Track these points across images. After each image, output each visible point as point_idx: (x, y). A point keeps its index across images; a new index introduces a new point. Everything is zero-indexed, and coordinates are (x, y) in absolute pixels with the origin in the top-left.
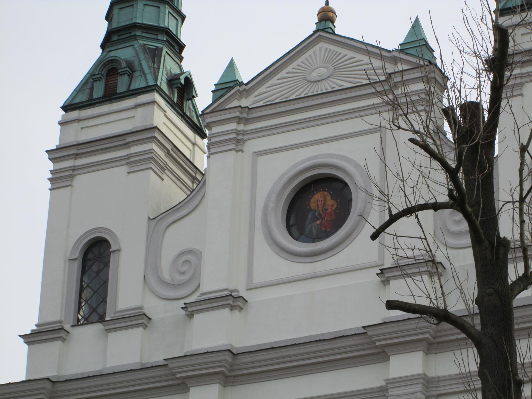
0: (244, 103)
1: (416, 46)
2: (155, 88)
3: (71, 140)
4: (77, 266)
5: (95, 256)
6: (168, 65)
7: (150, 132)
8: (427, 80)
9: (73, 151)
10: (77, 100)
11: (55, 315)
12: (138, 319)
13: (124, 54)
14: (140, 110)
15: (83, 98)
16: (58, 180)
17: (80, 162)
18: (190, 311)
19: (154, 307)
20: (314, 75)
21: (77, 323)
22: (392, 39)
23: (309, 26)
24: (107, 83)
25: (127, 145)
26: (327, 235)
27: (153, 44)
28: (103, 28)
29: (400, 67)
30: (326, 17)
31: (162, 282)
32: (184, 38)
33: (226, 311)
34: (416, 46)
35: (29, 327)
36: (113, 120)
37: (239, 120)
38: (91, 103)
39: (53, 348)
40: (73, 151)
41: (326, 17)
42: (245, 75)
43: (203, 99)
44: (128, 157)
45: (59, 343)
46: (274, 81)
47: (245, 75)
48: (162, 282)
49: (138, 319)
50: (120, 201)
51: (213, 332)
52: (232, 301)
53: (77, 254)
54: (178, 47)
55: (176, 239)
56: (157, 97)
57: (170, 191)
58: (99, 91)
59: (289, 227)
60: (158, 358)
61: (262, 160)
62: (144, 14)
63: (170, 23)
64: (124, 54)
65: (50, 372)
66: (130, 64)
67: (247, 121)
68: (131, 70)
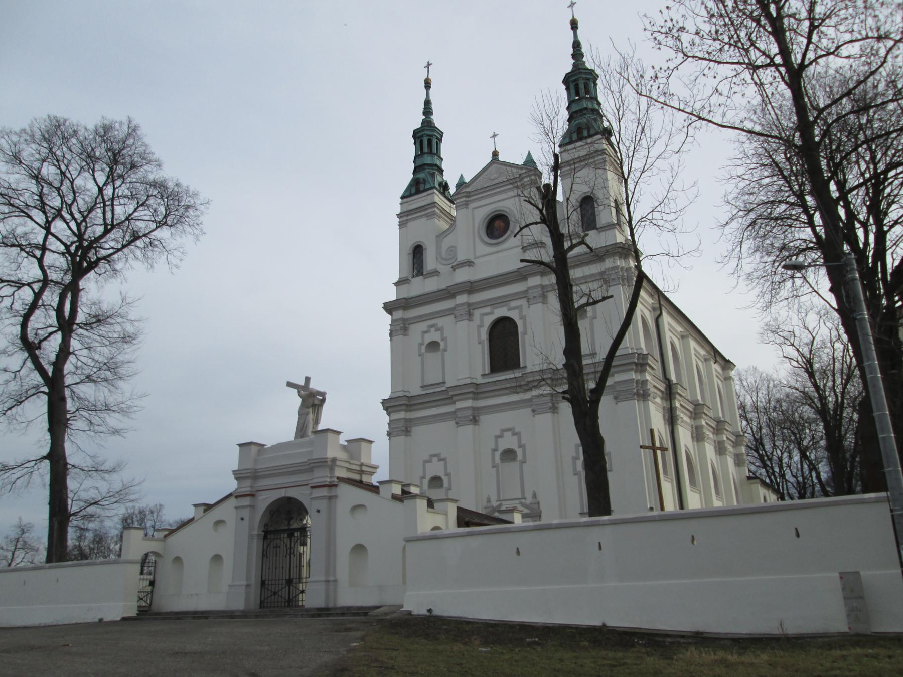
0: (467, 190)
1: (530, 162)
2: (434, 187)
3: (405, 210)
4: (411, 256)
5: (418, 252)
6: (438, 178)
7: (434, 204)
8: (535, 175)
11: (405, 275)
12: (435, 273)
13: (421, 175)
15: (408, 193)
16: (402, 225)
17: (409, 217)
18: (454, 268)
19: (440, 268)
20: (492, 177)
21: (413, 277)
23: (489, 159)
24: (416, 187)
27: (432, 171)
28: (413, 166)
30: (495, 154)
31: (443, 259)
32: (443, 168)
34: (530, 162)
35: (396, 280)
36: (419, 201)
37: (466, 196)
38: (411, 195)
39: (405, 287)
41: (495, 154)
42: (467, 180)
43: (452, 190)
48: (443, 259)
49: (435, 273)
50: (425, 231)
51: (463, 276)
52: (469, 263)
53: (411, 251)
54: (441, 171)
55: (446, 243)
56: (435, 191)
57: (444, 225)
58: (413, 191)
59: (487, 234)
60: (444, 287)
61: (476, 210)
62: (428, 160)
63: (437, 162)
64: (421, 175)
65: (405, 295)
66: (424, 179)
67: (469, 196)
68: (425, 181)
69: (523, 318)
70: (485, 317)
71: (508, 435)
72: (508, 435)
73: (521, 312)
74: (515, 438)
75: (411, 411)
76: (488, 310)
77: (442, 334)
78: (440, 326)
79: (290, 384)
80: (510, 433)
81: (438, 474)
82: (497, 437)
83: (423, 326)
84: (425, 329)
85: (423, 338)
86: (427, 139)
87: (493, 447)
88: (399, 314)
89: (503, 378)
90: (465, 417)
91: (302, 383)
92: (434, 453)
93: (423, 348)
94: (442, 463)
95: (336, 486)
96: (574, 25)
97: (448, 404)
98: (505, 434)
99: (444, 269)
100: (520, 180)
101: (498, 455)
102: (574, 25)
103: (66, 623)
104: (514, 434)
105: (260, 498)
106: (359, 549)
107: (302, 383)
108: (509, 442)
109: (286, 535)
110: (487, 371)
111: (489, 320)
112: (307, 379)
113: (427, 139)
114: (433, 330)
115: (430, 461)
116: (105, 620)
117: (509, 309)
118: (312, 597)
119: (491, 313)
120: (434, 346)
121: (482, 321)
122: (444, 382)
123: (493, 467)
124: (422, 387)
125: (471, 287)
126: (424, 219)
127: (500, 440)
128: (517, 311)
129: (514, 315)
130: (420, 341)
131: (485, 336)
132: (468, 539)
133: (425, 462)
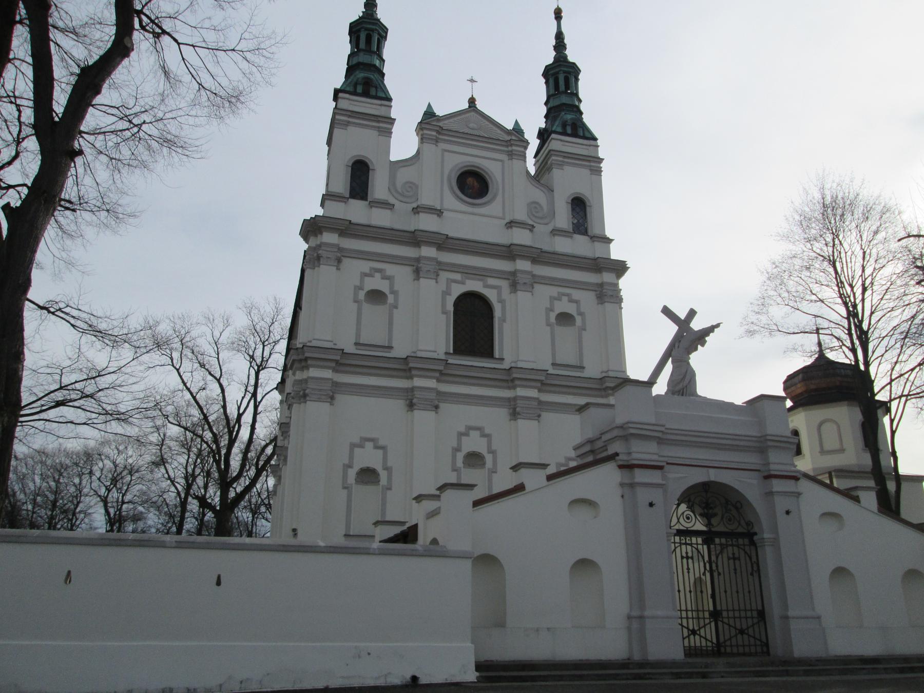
1: (518, 130)
9: (349, 113)
10: (348, 89)
14: (383, 108)
18: (416, 210)
20: (471, 125)
22: (510, 126)
25: (378, 122)
26: (470, 197)
29: (514, 138)
30: (472, 101)
33: (435, 216)
40: (349, 113)
41: (472, 101)
44: (379, 127)
45: (343, 204)
46: (451, 120)
47: (440, 111)
48: (396, 191)
51: (427, 223)
52: (439, 213)
61: (446, 154)
69: (501, 301)
70: (454, 285)
71: (474, 434)
72: (474, 434)
73: (499, 294)
74: (485, 439)
76: (458, 277)
77: (392, 286)
78: (388, 273)
79: (666, 311)
80: (477, 433)
81: (371, 465)
82: (461, 435)
83: (365, 266)
85: (362, 281)
86: (367, 34)
87: (455, 445)
88: (330, 238)
91: (682, 315)
92: (369, 436)
93: (362, 295)
94: (380, 452)
96: (558, 14)
97: (401, 377)
98: (472, 433)
99: (403, 208)
100: (507, 146)
101: (460, 457)
102: (558, 14)
104: (484, 435)
105: (671, 476)
106: (840, 572)
107: (682, 315)
108: (473, 443)
109: (700, 540)
110: (452, 351)
111: (458, 290)
112: (692, 313)
113: (367, 34)
114: (378, 275)
115: (361, 446)
116: (423, 680)
117: (486, 286)
119: (463, 283)
120: (376, 296)
122: (391, 348)
124: (356, 344)
125: (444, 243)
126: (375, 133)
127: (464, 439)
128: (495, 291)
129: (491, 295)
131: (450, 308)
133: (353, 446)
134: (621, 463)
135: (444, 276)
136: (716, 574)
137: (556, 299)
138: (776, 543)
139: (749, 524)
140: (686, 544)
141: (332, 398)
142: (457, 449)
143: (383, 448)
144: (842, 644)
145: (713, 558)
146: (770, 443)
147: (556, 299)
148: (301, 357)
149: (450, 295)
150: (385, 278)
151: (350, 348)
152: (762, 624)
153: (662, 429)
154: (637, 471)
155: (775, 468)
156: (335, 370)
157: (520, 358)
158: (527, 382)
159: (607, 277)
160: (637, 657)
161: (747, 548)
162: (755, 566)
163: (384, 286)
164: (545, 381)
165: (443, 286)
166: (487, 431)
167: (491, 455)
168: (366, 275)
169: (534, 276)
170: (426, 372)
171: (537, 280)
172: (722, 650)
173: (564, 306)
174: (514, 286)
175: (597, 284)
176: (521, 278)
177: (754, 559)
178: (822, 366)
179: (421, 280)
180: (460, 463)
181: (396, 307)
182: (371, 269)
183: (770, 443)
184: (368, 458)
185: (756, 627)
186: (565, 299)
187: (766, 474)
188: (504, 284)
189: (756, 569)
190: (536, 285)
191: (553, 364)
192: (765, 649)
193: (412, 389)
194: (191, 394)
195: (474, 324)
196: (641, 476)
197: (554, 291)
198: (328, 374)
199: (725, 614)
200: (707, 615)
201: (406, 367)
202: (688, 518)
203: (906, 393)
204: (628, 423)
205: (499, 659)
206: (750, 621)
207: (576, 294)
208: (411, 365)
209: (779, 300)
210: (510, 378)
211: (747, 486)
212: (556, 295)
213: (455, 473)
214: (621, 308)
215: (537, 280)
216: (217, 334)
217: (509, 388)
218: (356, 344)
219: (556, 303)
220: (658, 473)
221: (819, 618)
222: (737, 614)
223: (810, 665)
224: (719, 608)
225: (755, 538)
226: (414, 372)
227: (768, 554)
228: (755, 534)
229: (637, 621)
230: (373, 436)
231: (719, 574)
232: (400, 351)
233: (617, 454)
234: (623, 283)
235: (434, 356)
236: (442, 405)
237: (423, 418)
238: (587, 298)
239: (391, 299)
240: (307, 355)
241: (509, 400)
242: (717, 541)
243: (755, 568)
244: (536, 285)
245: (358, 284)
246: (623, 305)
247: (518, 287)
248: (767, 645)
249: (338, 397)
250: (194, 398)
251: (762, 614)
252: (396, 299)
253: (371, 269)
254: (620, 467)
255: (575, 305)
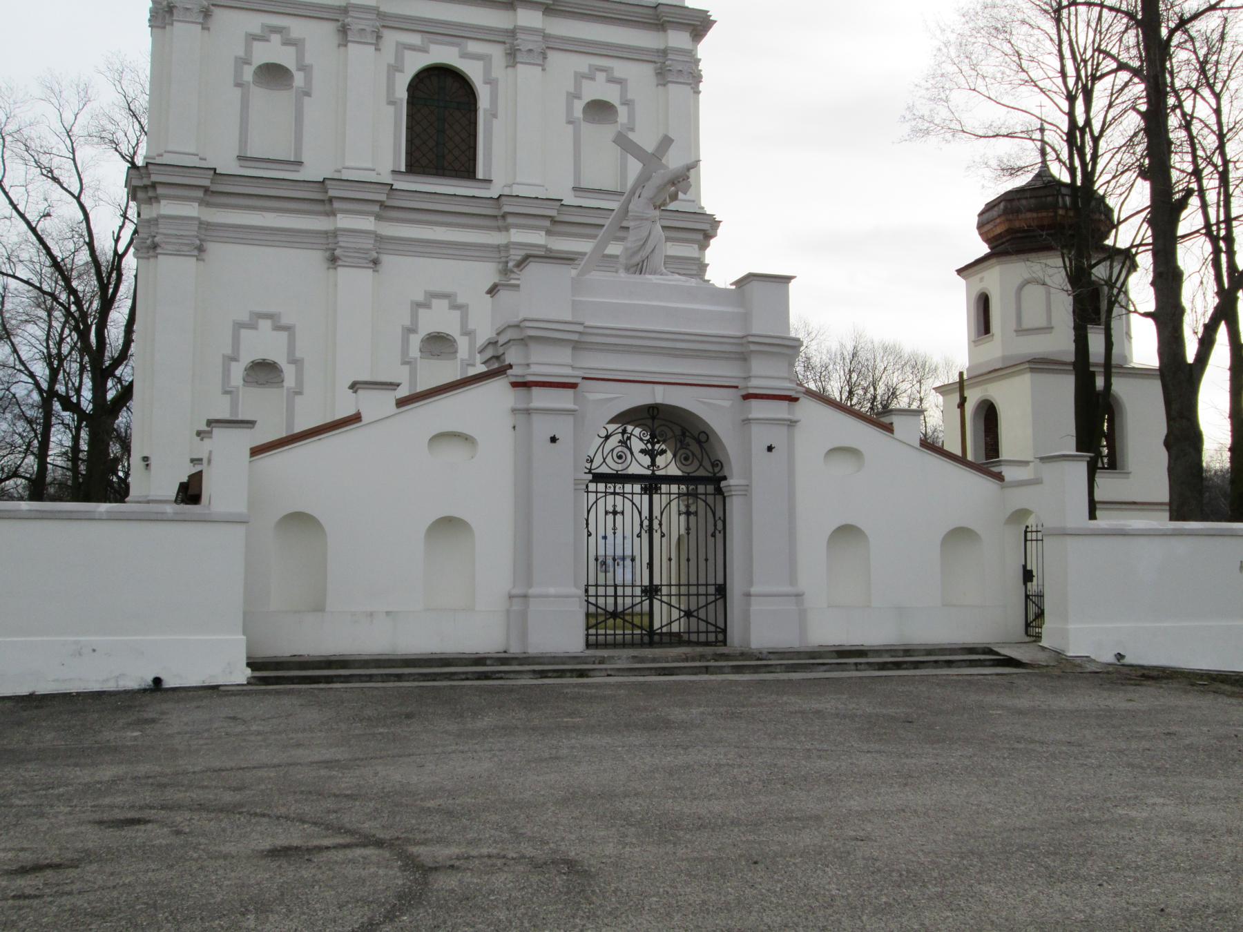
69: (490, 82)
70: (408, 54)
72: (440, 305)
73: (487, 70)
74: (457, 313)
75: (208, 204)
76: (415, 39)
77: (300, 56)
80: (445, 303)
81: (271, 356)
82: (419, 305)
84: (257, 30)
89: (451, 190)
90: (358, 250)
93: (248, 74)
94: (284, 335)
95: (796, 399)
98: (435, 302)
101: (415, 341)
103: (110, 686)
105: (591, 397)
106: (847, 534)
109: (637, 488)
110: (403, 169)
111: (415, 63)
114: (276, 38)
115: (252, 326)
118: (760, 625)
119: (425, 51)
120: (274, 74)
121: (399, 57)
123: (404, 363)
124: (240, 158)
127: (421, 311)
129: (473, 71)
130: (241, 53)
131: (402, 94)
132: (1174, 542)
133: (239, 326)
134: (514, 380)
135: (391, 38)
136: (657, 536)
137: (584, 76)
138: (746, 490)
139: (718, 464)
140: (614, 493)
141: (201, 249)
142: (411, 330)
143: (288, 328)
144: (829, 630)
145: (656, 513)
146: (753, 347)
147: (584, 76)
148: (146, 182)
149: (402, 71)
150: (287, 42)
151: (227, 165)
152: (720, 603)
153: (580, 328)
154: (535, 390)
155: (757, 384)
156: (203, 203)
157: (518, 180)
158: (529, 219)
159: (677, 39)
160: (515, 649)
161: (710, 499)
162: (720, 524)
163: (286, 57)
164: (556, 218)
165: (388, 54)
166: (460, 300)
167: (466, 338)
168: (255, 38)
169: (546, 37)
170: (358, 204)
171: (551, 44)
172: (656, 638)
173: (598, 90)
174: (512, 56)
175: (658, 51)
176: (524, 42)
177: (719, 513)
178: (1044, 185)
179: (350, 45)
180: (414, 351)
181: (308, 94)
182: (264, 26)
183: (753, 347)
184: (264, 344)
185: (711, 607)
186: (601, 77)
187: (744, 393)
188: (497, 53)
189: (720, 527)
190: (550, 54)
191: (576, 189)
192: (720, 637)
193: (335, 234)
194: (28, 223)
195: (442, 118)
196: (540, 398)
197: (582, 63)
198: (191, 210)
199: (665, 590)
200: (638, 591)
201: (323, 196)
202: (620, 457)
203: (1137, 242)
204: (525, 320)
205: (317, 653)
206: (702, 599)
207: (621, 68)
208: (331, 193)
209: (962, 81)
210: (499, 213)
211: (713, 410)
212: (585, 70)
213: (407, 367)
214: (698, 92)
215: (551, 44)
216: (68, 117)
217: (499, 229)
218: (240, 158)
219: (586, 84)
220: (569, 393)
221: (799, 595)
222: (693, 590)
223: (759, 659)
224: (656, 581)
225: (723, 484)
226: (336, 205)
227: (735, 507)
228: (725, 478)
229: (520, 599)
230: (272, 309)
231: (663, 536)
232: (313, 171)
233: (510, 366)
234: (706, 49)
235: (372, 177)
236: (385, 259)
237: (354, 281)
238: (639, 75)
239: (299, 79)
240: (154, 178)
241: (498, 248)
242: (664, 488)
243: (720, 524)
244: (550, 54)
245: (241, 53)
246: (702, 86)
247: (520, 58)
248: (724, 631)
249: (213, 248)
250: (34, 230)
251: (721, 591)
252: (308, 80)
253: (264, 26)
254: (515, 385)
255: (618, 87)
